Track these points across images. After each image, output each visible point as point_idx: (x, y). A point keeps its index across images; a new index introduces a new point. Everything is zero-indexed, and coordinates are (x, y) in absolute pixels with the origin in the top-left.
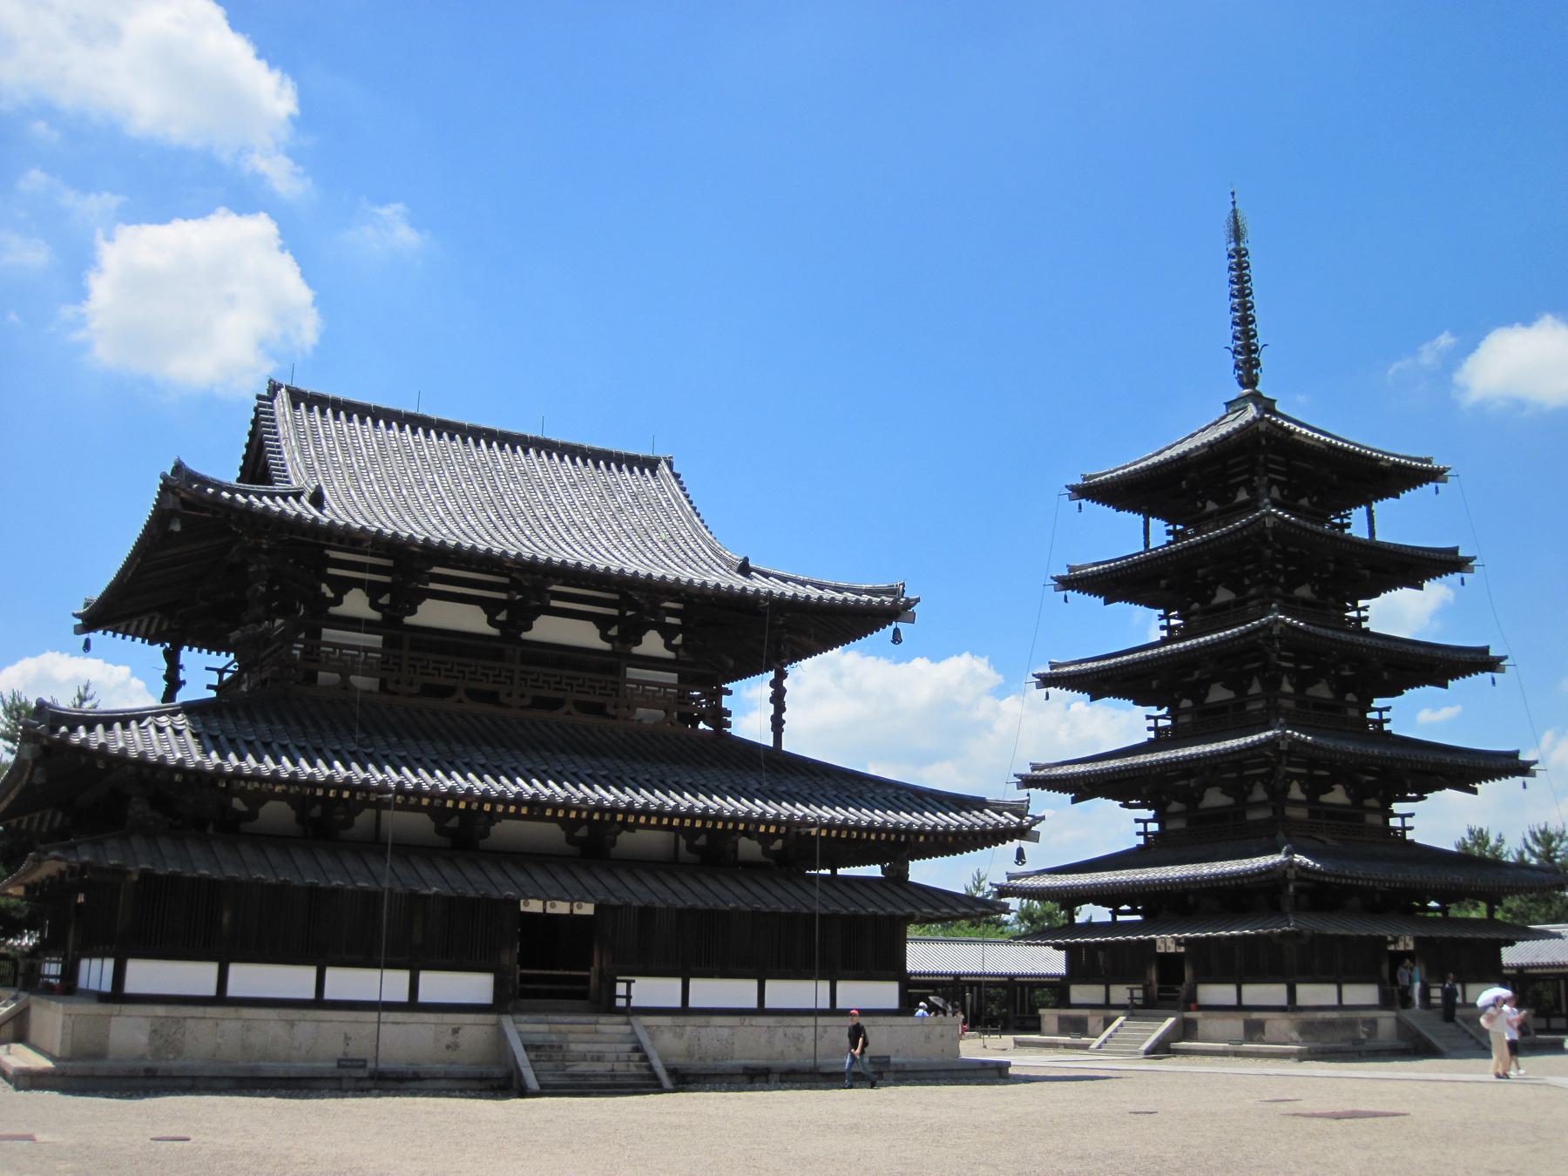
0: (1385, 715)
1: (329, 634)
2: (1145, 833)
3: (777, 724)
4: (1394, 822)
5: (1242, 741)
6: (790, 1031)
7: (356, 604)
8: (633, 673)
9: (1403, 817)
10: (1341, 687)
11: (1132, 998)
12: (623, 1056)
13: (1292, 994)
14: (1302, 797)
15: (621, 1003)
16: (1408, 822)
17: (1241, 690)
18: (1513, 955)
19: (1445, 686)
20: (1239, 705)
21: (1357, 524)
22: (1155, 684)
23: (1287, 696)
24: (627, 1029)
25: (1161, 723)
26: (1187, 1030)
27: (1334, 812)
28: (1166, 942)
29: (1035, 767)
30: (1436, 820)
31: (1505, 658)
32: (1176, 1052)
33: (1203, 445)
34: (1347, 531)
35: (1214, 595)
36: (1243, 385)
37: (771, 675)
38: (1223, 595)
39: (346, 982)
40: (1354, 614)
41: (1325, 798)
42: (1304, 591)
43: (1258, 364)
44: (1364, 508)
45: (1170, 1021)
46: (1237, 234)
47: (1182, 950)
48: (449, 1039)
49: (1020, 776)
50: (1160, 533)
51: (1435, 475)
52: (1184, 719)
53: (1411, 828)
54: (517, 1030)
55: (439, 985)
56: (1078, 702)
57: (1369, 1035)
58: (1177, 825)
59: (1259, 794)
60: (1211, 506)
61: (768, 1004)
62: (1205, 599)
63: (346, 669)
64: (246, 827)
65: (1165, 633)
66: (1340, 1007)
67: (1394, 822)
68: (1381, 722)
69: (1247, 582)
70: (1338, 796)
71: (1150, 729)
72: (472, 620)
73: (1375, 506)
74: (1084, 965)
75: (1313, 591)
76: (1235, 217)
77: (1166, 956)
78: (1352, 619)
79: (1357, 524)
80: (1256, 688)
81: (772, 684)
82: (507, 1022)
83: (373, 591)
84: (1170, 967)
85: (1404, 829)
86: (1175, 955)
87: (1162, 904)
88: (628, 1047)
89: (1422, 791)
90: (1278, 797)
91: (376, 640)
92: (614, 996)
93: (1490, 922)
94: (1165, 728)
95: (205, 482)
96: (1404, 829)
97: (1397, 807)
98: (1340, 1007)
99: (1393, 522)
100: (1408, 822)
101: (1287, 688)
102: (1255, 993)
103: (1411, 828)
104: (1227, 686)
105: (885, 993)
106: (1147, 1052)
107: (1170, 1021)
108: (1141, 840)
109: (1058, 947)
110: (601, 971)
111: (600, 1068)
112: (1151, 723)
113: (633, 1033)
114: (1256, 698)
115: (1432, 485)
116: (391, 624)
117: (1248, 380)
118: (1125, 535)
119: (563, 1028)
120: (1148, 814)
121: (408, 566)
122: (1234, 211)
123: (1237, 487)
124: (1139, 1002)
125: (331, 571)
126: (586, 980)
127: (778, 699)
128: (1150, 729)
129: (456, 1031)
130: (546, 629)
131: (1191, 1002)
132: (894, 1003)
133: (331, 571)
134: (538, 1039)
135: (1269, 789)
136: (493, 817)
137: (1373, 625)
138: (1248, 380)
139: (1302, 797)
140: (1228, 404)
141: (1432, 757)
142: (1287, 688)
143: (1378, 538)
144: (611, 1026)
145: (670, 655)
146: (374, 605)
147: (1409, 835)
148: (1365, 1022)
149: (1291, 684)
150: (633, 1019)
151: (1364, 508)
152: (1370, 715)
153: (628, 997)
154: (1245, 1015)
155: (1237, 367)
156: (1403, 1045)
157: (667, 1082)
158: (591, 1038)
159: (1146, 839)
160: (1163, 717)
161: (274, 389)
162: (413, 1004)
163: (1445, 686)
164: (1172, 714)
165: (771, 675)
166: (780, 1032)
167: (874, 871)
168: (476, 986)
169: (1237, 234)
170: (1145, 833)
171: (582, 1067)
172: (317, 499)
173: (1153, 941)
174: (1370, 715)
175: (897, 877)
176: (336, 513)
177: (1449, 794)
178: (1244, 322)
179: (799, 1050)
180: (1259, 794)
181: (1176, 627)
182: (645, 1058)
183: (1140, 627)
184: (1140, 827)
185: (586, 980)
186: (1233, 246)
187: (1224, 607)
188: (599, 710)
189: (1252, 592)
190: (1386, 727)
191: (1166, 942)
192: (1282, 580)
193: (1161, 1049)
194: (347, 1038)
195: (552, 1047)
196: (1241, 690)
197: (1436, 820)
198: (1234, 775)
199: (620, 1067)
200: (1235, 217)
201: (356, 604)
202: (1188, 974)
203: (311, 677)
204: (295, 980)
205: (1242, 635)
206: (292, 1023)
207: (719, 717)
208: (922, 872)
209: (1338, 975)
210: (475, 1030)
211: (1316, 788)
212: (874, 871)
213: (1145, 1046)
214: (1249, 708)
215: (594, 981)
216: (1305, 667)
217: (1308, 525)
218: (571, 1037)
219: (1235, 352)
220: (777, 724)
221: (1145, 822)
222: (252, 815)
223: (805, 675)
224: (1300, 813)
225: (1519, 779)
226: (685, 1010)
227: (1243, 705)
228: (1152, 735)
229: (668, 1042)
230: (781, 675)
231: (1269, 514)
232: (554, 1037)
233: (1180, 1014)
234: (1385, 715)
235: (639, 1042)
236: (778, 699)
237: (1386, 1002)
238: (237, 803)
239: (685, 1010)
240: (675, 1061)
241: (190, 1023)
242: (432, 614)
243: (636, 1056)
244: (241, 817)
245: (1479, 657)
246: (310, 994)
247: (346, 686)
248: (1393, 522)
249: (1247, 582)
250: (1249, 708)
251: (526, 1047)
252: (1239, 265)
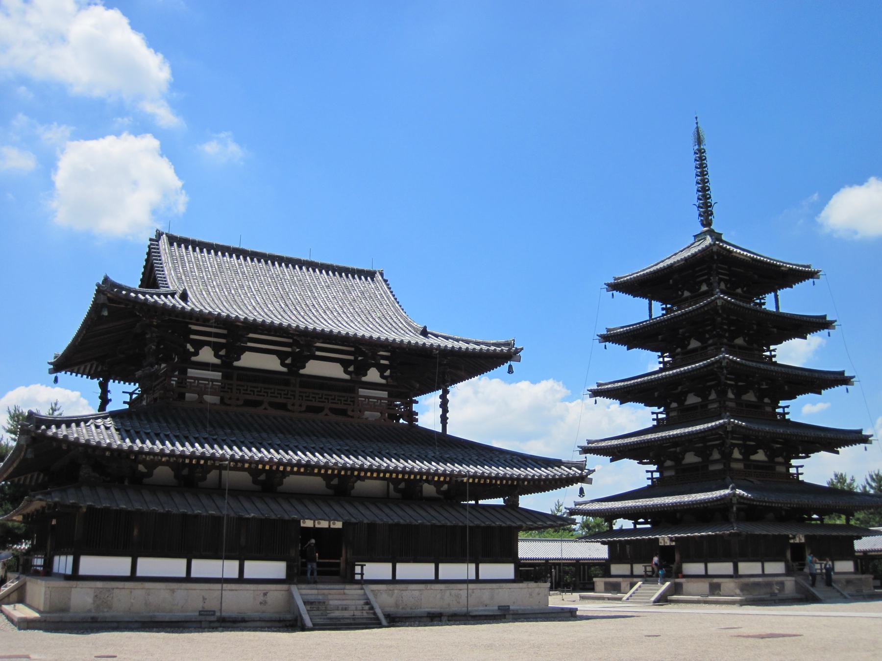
0: (786, 410)
1: (192, 372)
2: (652, 479)
3: (444, 419)
4: (792, 470)
5: (706, 426)
6: (453, 592)
7: (206, 355)
8: (363, 392)
9: (797, 467)
10: (761, 394)
11: (646, 571)
12: (360, 607)
13: (736, 568)
14: (740, 457)
15: (358, 577)
16: (800, 470)
17: (705, 396)
18: (861, 545)
19: (820, 393)
20: (703, 406)
21: (769, 303)
22: (656, 394)
23: (731, 400)
24: (361, 592)
25: (660, 416)
26: (677, 589)
27: (758, 465)
28: (665, 539)
29: (589, 442)
30: (816, 469)
31: (854, 377)
32: (671, 601)
33: (682, 260)
34: (763, 307)
35: (689, 344)
36: (704, 225)
37: (440, 392)
38: (694, 344)
39: (203, 567)
40: (768, 353)
41: (753, 457)
42: (739, 341)
43: (712, 214)
44: (773, 294)
45: (668, 584)
46: (699, 141)
47: (674, 544)
48: (261, 598)
49: (581, 447)
50: (658, 309)
51: (811, 275)
52: (672, 414)
53: (802, 474)
54: (300, 593)
55: (255, 568)
56: (614, 404)
57: (780, 590)
59: (716, 455)
60: (687, 294)
61: (441, 577)
62: (684, 346)
63: (201, 392)
64: (146, 481)
65: (661, 366)
66: (763, 575)
67: (792, 470)
68: (784, 414)
69: (707, 336)
70: (760, 456)
71: (654, 420)
72: (272, 363)
73: (779, 292)
74: (619, 553)
75: (745, 340)
76: (698, 131)
77: (665, 548)
78: (767, 356)
79: (769, 303)
80: (713, 396)
81: (441, 397)
82: (294, 589)
83: (216, 348)
84: (666, 554)
85: (798, 474)
86: (670, 546)
87: (661, 518)
88: (362, 602)
89: (808, 453)
90: (727, 457)
91: (217, 375)
92: (353, 574)
93: (847, 526)
94: (662, 419)
95: (121, 288)
96: (798, 474)
97: (794, 462)
98: (763, 575)
99: (789, 301)
100: (800, 470)
101: (731, 395)
102: (715, 568)
103: (802, 474)
104: (697, 395)
105: (507, 570)
106: (655, 602)
107: (668, 584)
108: (649, 482)
109: (603, 543)
110: (346, 560)
111: (346, 614)
112: (655, 416)
113: (365, 594)
114: (713, 401)
115: (811, 280)
116: (226, 366)
117: (707, 223)
118: (638, 311)
119: (326, 592)
120: (654, 467)
121: (235, 333)
122: (697, 128)
123: (701, 283)
124: (650, 574)
125: (192, 337)
126: (338, 565)
127: (444, 405)
128: (654, 420)
129: (265, 594)
130: (314, 368)
131: (679, 573)
132: (511, 576)
133: (192, 337)
134: (312, 598)
135: (722, 453)
136: (285, 474)
137: (779, 360)
138: (707, 223)
139: (740, 457)
140: (695, 236)
141: (812, 433)
142: (731, 395)
143: (781, 310)
144: (352, 591)
145: (383, 381)
146: (216, 355)
147: (801, 478)
148: (778, 583)
149: (733, 393)
150: (364, 586)
151: (773, 294)
152: (777, 410)
153: (362, 574)
154: (710, 580)
155: (700, 215)
156: (799, 596)
157: (384, 622)
158: (341, 597)
159: (653, 482)
160: (661, 413)
161: (159, 235)
162: (241, 580)
163: (820, 393)
164: (666, 411)
165: (440, 392)
166: (448, 593)
167: (500, 501)
168: (276, 569)
169: (699, 141)
170: (652, 479)
171: (337, 614)
172: (184, 297)
173: (657, 539)
174: (777, 410)
175: (512, 505)
176: (195, 304)
177: (823, 455)
179: (459, 603)
180: (716, 455)
181: (668, 362)
182: (372, 608)
183: (647, 363)
184: (649, 475)
185: (338, 565)
186: (697, 147)
187: (695, 350)
188: (343, 413)
189: (710, 342)
190: (787, 417)
191: (665, 539)
192: (727, 335)
193: (663, 600)
194: (204, 599)
195: (319, 603)
196: (705, 397)
197: (816, 469)
198: (701, 445)
199: (358, 614)
200: (698, 131)
201: (206, 355)
202: (677, 557)
203: (182, 396)
204: (175, 567)
205: (705, 366)
206: (173, 591)
207: (411, 416)
208: (527, 502)
209: (762, 558)
210: (276, 594)
211: (748, 452)
212: (500, 501)
213: (653, 599)
215: (342, 566)
216: (740, 384)
217: (741, 304)
218: (330, 597)
219: (699, 207)
220: (444, 419)
221: (652, 472)
222: (149, 474)
223: (459, 391)
224: (739, 466)
225: (863, 445)
226: (394, 581)
227: (706, 405)
228: (655, 423)
229: (385, 600)
230: (446, 392)
231: (719, 298)
232: (320, 597)
233: (673, 580)
234: (786, 410)
235: (368, 599)
236: (444, 405)
237: (789, 572)
238: (141, 468)
239: (394, 581)
240: (388, 609)
242: (249, 360)
243: (367, 607)
244: (144, 475)
245: (839, 377)
246: (183, 574)
247: (201, 401)
248: (789, 301)
249: (707, 336)
250: (710, 407)
251: (305, 603)
252: (700, 158)
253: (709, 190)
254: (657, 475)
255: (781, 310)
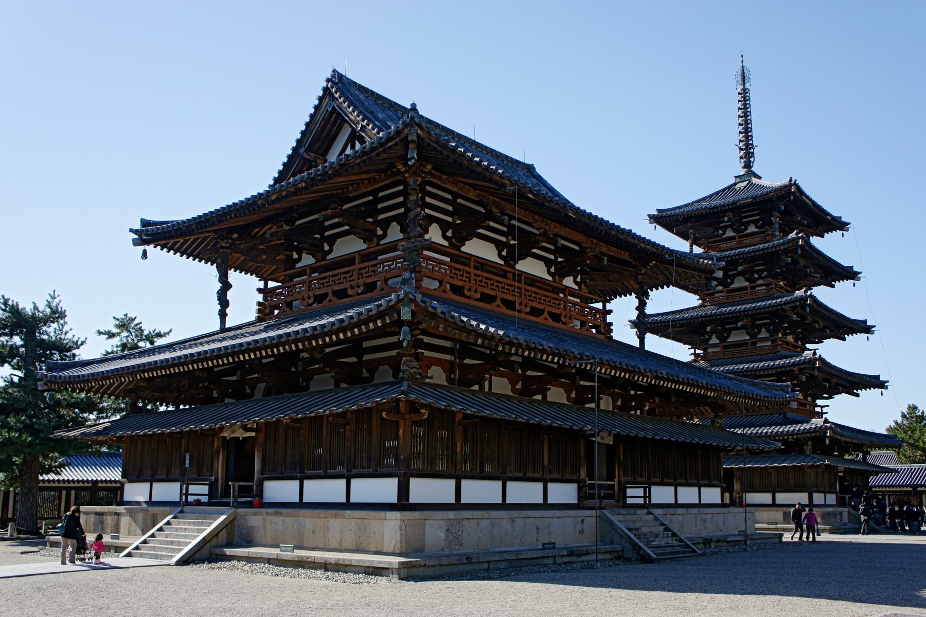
9: (822, 407)
67: (818, 409)
76: (743, 73)
89: (832, 393)
97: (819, 402)
99: (828, 244)
100: (825, 410)
123: (749, 223)
178: (747, 131)
197: (840, 410)
206: (513, 520)
214: (758, 345)
227: (754, 344)
241: (465, 522)
248: (828, 244)
250: (758, 345)
253: (751, 131)
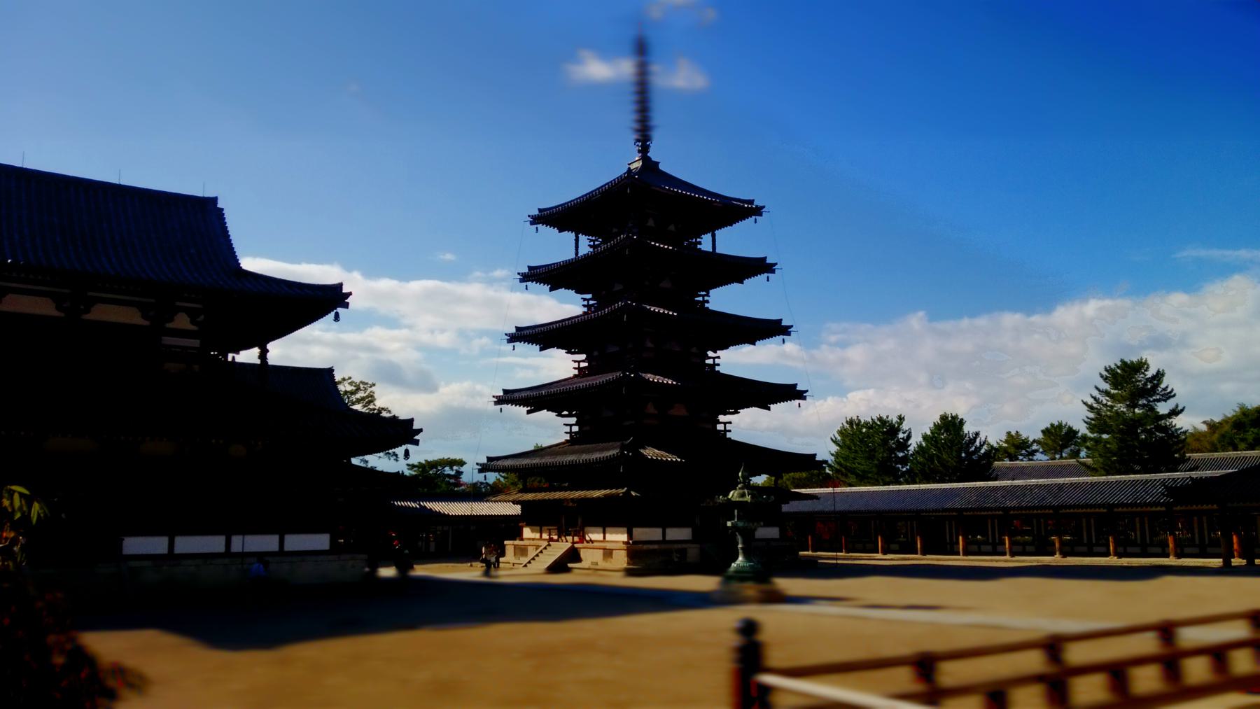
0: (717, 361)
2: (570, 433)
4: (720, 427)
9: (725, 423)
18: (785, 508)
21: (705, 243)
25: (583, 365)
40: (700, 299)
56: (529, 351)
58: (587, 428)
66: (664, 541)
67: (720, 427)
68: (715, 364)
96: (726, 431)
97: (722, 418)
98: (664, 541)
99: (731, 241)
108: (568, 437)
112: (576, 365)
117: (644, 150)
118: (561, 247)
120: (573, 420)
138: (644, 150)
143: (718, 251)
147: (729, 435)
151: (709, 235)
152: (708, 361)
170: (570, 433)
174: (708, 361)
184: (568, 429)
190: (717, 368)
197: (746, 425)
221: (571, 426)
225: (797, 402)
228: (576, 372)
254: (575, 429)
255: (718, 251)
